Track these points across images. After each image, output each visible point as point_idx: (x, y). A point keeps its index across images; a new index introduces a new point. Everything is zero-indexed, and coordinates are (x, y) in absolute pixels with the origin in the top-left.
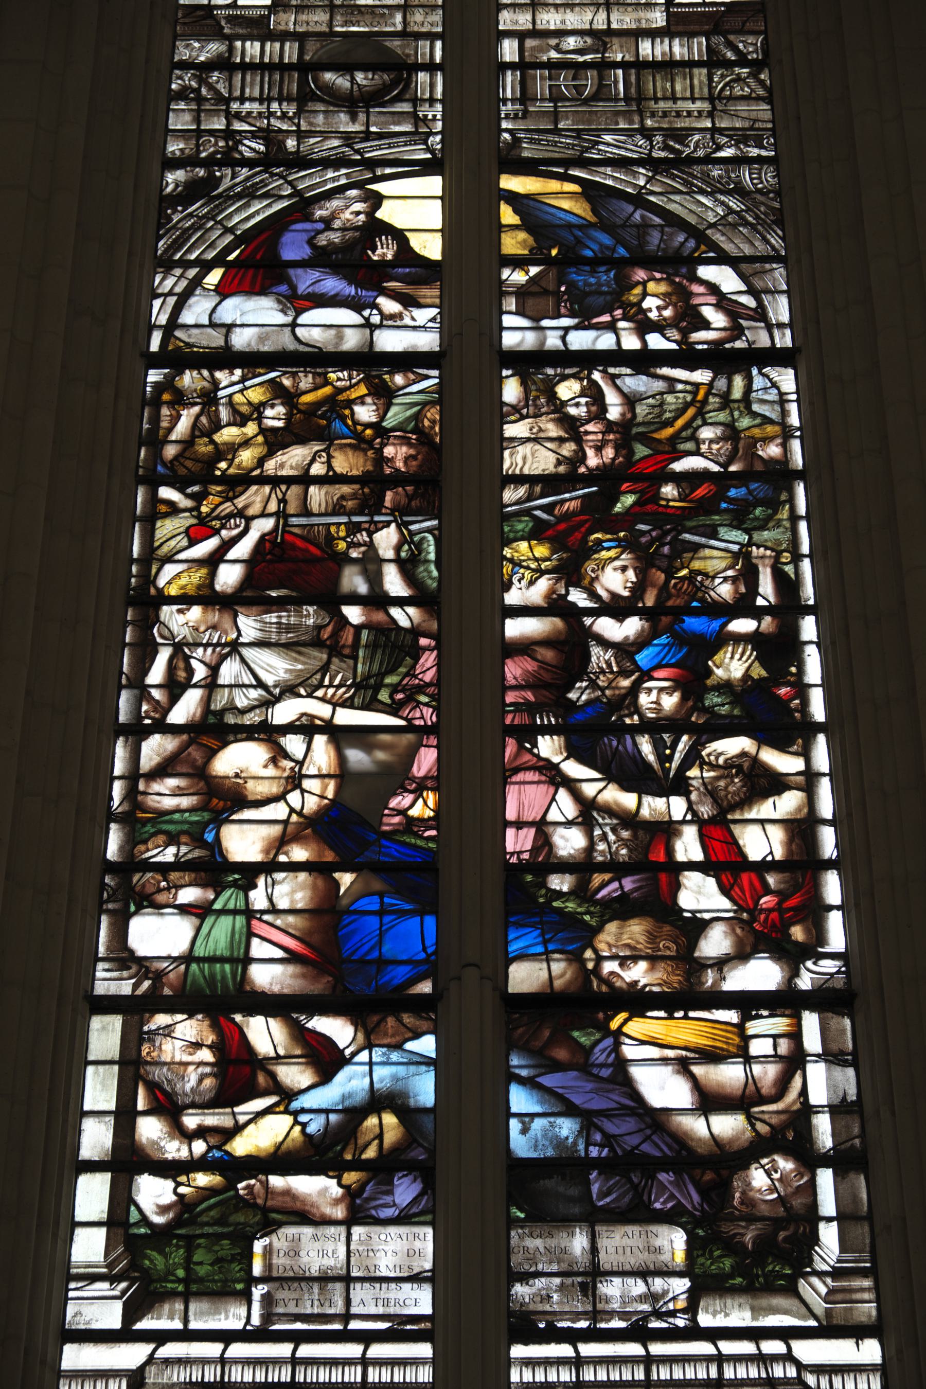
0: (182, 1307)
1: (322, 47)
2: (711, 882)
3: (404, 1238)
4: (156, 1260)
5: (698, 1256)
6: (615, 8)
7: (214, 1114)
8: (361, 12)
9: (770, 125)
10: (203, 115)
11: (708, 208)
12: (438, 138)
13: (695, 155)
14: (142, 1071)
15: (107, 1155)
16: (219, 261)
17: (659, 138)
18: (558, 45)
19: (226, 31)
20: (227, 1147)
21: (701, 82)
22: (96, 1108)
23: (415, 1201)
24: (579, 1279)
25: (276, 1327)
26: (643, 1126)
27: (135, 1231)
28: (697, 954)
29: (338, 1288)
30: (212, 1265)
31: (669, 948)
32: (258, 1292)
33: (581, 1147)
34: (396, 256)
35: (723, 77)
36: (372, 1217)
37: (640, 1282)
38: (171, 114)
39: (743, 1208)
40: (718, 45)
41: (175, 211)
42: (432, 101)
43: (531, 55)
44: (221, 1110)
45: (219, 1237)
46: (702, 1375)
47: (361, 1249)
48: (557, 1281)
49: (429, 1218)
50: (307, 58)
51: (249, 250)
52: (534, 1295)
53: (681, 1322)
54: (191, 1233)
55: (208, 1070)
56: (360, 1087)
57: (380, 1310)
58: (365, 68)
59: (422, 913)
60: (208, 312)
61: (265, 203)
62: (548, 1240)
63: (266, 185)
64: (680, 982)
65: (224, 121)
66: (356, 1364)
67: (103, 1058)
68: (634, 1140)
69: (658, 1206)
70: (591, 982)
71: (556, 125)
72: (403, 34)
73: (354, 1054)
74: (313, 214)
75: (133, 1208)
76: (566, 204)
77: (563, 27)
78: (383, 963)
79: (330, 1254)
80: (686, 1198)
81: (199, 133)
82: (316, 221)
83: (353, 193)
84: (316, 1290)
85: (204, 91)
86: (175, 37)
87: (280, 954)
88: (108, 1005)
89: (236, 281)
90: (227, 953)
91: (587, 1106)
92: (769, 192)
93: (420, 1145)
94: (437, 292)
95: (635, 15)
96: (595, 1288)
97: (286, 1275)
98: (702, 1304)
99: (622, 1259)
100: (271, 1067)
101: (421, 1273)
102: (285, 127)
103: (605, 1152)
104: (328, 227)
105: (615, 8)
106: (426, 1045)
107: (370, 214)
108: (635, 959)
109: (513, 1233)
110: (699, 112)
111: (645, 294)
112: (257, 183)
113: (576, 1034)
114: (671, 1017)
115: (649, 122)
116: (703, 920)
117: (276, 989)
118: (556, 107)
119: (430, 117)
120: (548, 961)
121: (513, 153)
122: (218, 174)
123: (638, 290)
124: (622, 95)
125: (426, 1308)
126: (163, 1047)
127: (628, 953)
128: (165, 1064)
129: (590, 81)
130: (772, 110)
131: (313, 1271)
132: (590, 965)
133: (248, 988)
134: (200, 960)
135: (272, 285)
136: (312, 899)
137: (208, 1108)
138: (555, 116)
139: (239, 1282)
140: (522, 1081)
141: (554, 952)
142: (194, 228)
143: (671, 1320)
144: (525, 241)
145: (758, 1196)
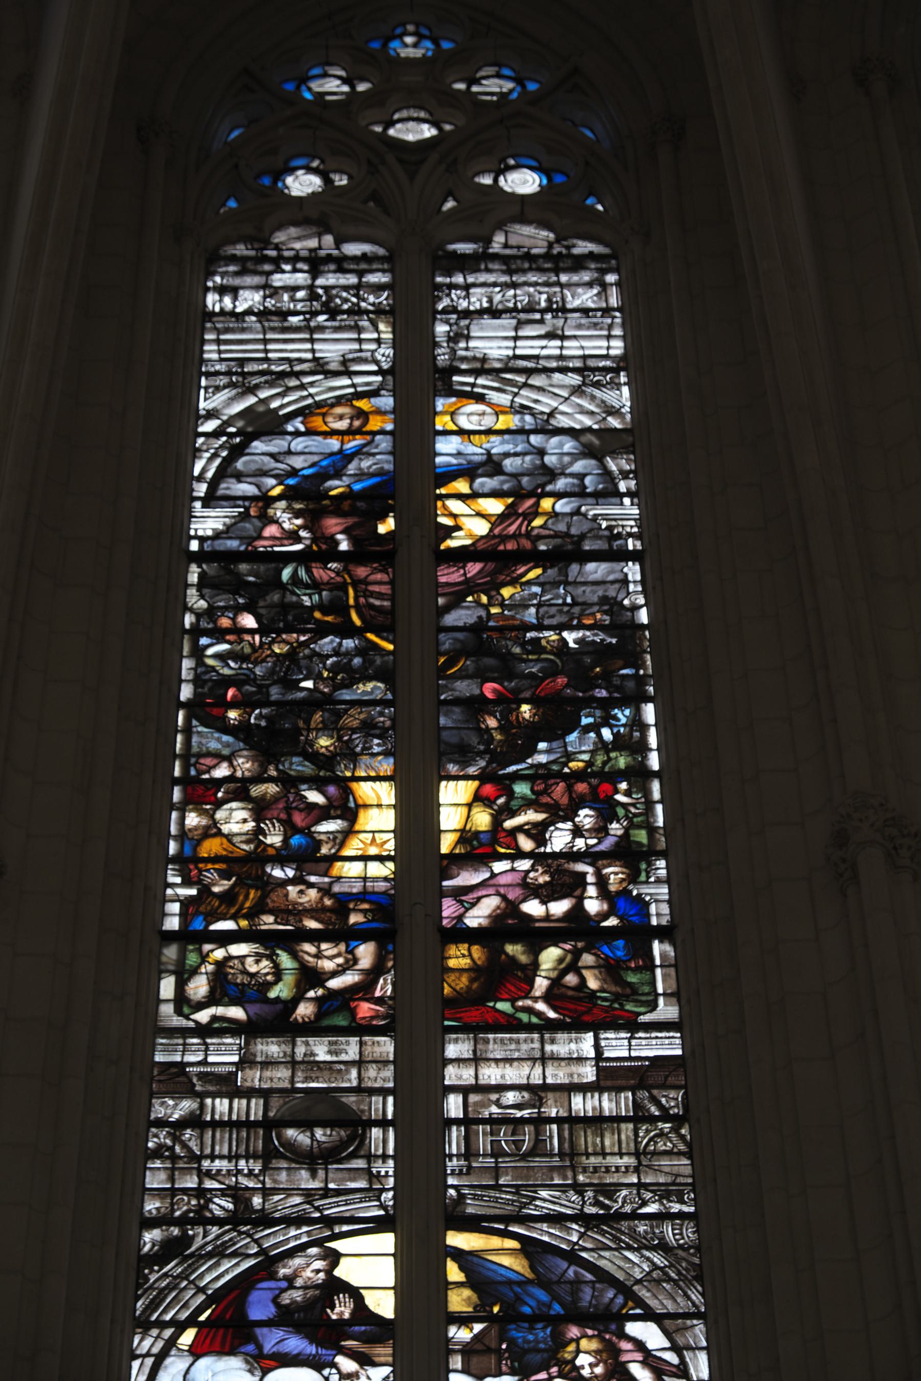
1: (285, 1103)
6: (549, 1063)
8: (320, 1069)
9: (690, 1180)
10: (176, 1173)
11: (635, 1264)
12: (390, 1194)
13: (623, 1210)
16: (191, 1321)
17: (590, 1194)
18: (498, 1100)
19: (198, 1088)
21: (627, 1137)
34: (353, 1314)
35: (647, 1131)
38: (148, 1173)
41: (152, 1271)
42: (385, 1157)
43: (475, 1111)
50: (271, 1114)
51: (219, 1310)
58: (324, 1124)
60: (183, 1373)
61: (234, 1261)
63: (234, 1244)
65: (196, 1179)
71: (497, 1181)
74: (277, 1272)
76: (506, 1261)
77: (502, 1082)
81: (173, 1191)
82: (280, 1280)
83: (313, 1251)
85: (178, 1149)
86: (152, 1095)
89: (208, 1341)
92: (690, 1247)
94: (389, 1351)
95: (568, 1070)
102: (251, 1185)
104: (291, 1286)
105: (549, 1063)
107: (329, 1272)
110: (626, 1167)
111: (578, 1351)
112: (226, 1242)
115: (581, 1178)
118: (497, 1162)
119: (383, 1173)
121: (458, 1209)
122: (190, 1232)
123: (572, 1348)
124: (556, 1151)
129: (527, 1136)
130: (692, 1164)
135: (241, 1345)
138: (496, 1172)
142: (170, 1288)
144: (469, 1298)
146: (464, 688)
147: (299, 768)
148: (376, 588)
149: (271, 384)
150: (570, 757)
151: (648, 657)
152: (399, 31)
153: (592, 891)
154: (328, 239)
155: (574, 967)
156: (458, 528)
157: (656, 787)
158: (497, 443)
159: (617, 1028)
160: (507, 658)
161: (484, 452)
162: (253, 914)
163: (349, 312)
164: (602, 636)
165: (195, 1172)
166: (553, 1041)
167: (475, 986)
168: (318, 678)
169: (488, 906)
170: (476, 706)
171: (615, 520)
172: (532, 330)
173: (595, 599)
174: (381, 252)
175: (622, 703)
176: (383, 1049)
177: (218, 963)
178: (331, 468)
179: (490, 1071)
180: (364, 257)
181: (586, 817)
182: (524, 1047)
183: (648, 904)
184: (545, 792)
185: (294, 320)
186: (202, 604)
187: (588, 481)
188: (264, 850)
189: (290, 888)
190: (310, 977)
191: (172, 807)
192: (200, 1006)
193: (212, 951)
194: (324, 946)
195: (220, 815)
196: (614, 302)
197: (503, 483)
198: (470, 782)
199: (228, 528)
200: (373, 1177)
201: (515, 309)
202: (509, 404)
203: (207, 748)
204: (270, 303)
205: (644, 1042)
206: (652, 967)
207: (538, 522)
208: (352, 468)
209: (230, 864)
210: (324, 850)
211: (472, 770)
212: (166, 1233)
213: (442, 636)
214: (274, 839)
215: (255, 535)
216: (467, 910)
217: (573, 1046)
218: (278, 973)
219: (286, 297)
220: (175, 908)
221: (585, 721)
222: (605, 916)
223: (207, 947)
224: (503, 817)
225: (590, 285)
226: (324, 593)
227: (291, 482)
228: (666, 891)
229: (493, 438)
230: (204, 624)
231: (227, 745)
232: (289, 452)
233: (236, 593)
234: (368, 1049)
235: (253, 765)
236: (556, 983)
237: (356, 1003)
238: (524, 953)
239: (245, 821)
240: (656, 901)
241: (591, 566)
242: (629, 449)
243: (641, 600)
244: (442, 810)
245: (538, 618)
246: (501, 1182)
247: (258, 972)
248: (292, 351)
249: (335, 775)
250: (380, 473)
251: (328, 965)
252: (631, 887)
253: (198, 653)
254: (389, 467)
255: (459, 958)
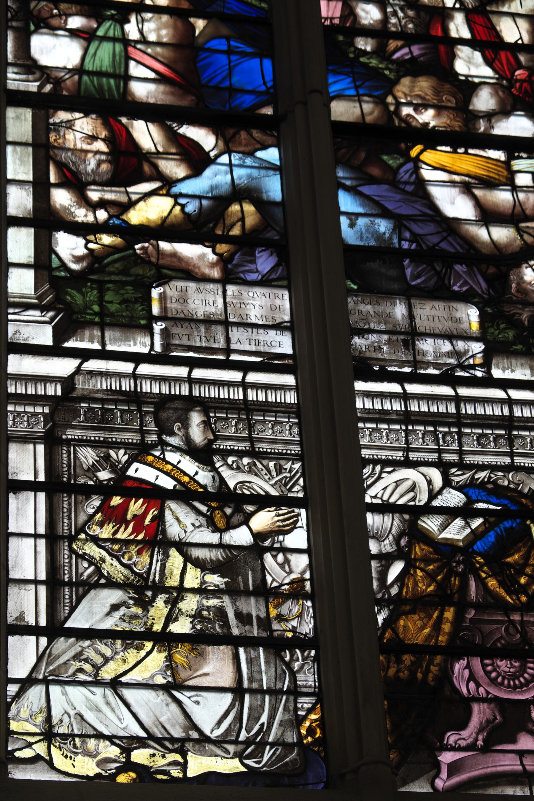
0: (99, 334)
2: (478, 56)
3: (267, 296)
4: (76, 297)
5: (489, 327)
7: (111, 191)
14: (51, 153)
15: (29, 214)
20: (124, 217)
22: (18, 177)
23: (273, 270)
24: (402, 337)
25: (174, 354)
26: (440, 230)
27: (58, 274)
28: (471, 107)
29: (219, 330)
30: (120, 304)
31: (450, 101)
32: (158, 327)
33: (395, 241)
36: (241, 279)
37: (447, 343)
39: (519, 295)
44: (117, 189)
45: (126, 283)
46: (498, 412)
47: (234, 301)
48: (385, 337)
49: (285, 283)
52: (369, 346)
53: (479, 374)
54: (101, 279)
55: (103, 157)
56: (224, 181)
57: (253, 348)
59: (261, 56)
62: (376, 306)
64: (460, 127)
66: (238, 386)
67: (19, 140)
68: (435, 239)
69: (456, 288)
70: (393, 120)
73: (217, 156)
75: (53, 256)
78: (233, 91)
79: (211, 303)
80: (476, 285)
84: (203, 329)
87: (152, 75)
88: (20, 99)
90: (110, 70)
91: (397, 211)
93: (273, 229)
96: (414, 345)
97: (178, 316)
98: (494, 362)
99: (432, 325)
100: (153, 160)
101: (282, 323)
103: (414, 246)
106: (272, 155)
108: (426, 106)
109: (349, 300)
113: (385, 158)
114: (455, 152)
116: (473, 83)
117: (152, 101)
120: (360, 102)
125: (287, 348)
126: (67, 137)
127: (419, 102)
128: (69, 149)
131: (199, 315)
132: (392, 108)
133: (130, 99)
134: (90, 73)
136: (174, 36)
137: (107, 186)
139: (143, 319)
140: (347, 189)
141: (364, 95)
143: (472, 371)
145: (529, 287)
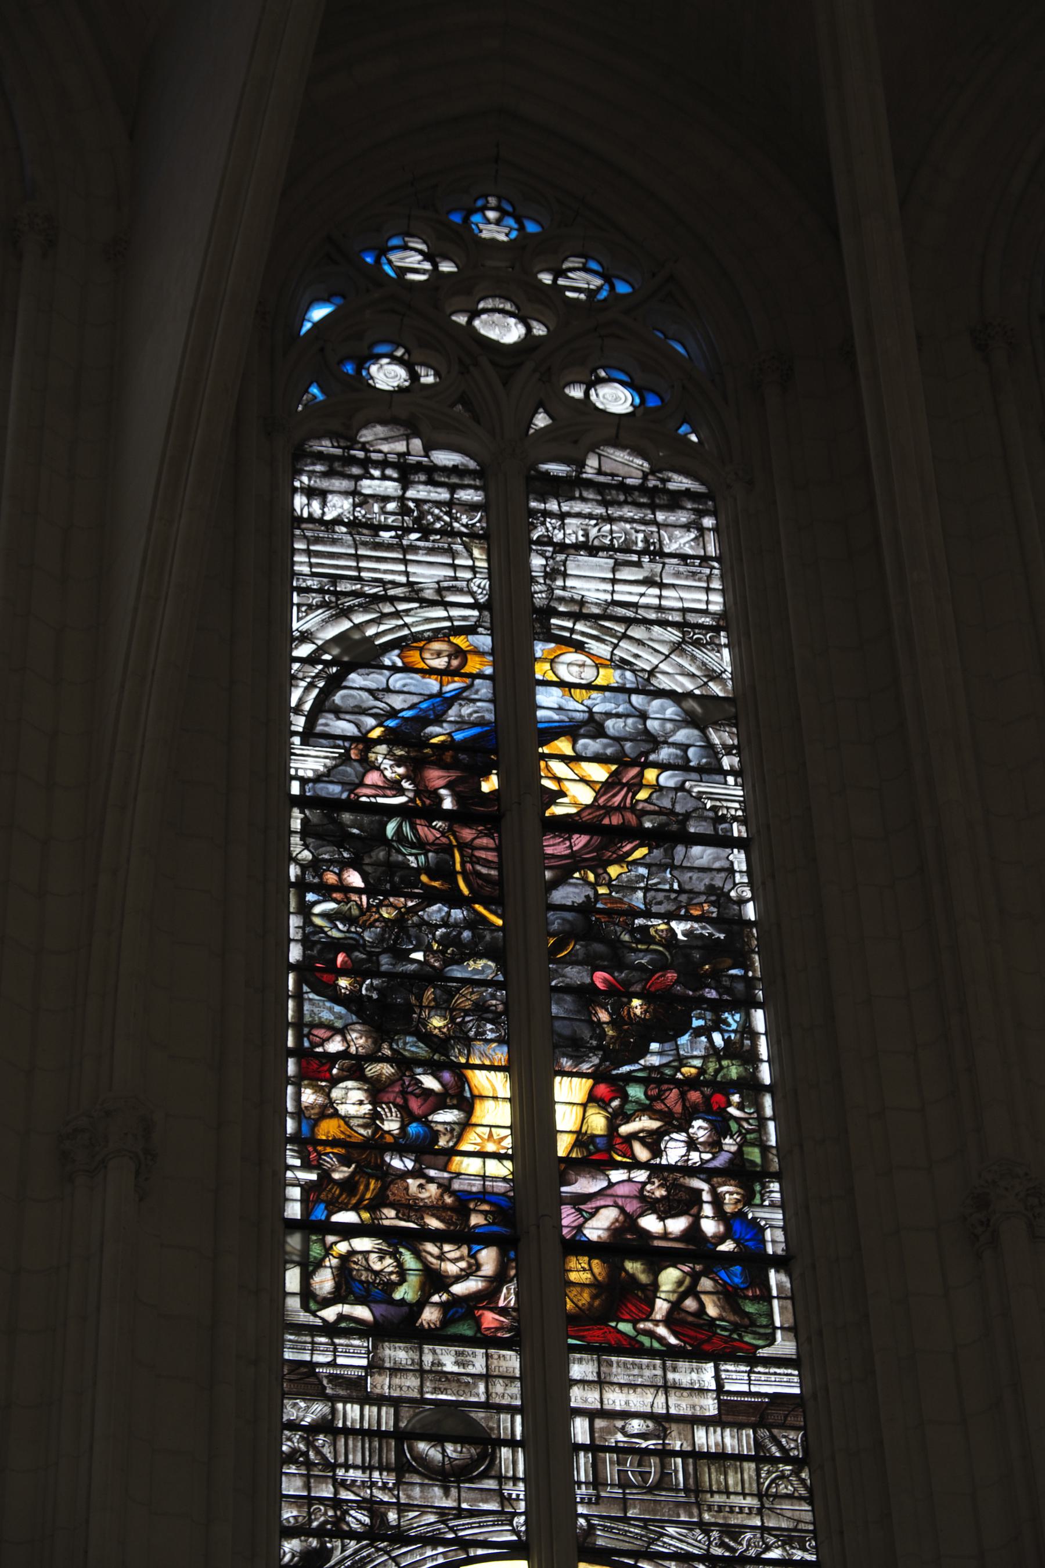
6: (672, 1392)
8: (447, 1379)
9: (811, 1527)
10: (312, 1481)
12: (522, 1519)
17: (715, 1534)
18: (623, 1427)
19: (329, 1391)
21: (750, 1477)
35: (769, 1473)
38: (284, 1478)
40: (764, 1438)
42: (515, 1479)
43: (601, 1437)
50: (402, 1425)
58: (454, 1440)
63: (372, 1561)
65: (332, 1489)
71: (625, 1513)
72: (487, 1406)
77: (627, 1409)
86: (284, 1395)
102: (386, 1499)
105: (672, 1392)
110: (750, 1508)
112: (364, 1558)
115: (706, 1516)
118: (624, 1493)
121: (588, 1540)
122: (329, 1545)
124: (682, 1486)
130: (813, 1511)
138: (624, 1503)
146: (575, 975)
147: (413, 1049)
148: (482, 854)
149: (365, 608)
150: (682, 1061)
151: (757, 957)
152: (480, 203)
153: (708, 1210)
154: (417, 444)
155: (692, 1291)
156: (562, 794)
157: (768, 1101)
158: (597, 701)
159: (737, 1360)
160: (616, 944)
161: (586, 709)
162: (375, 1206)
163: (441, 532)
164: (710, 930)
165: (330, 1481)
166: (675, 1370)
167: (597, 1303)
168: (428, 950)
169: (607, 1218)
170: (587, 996)
171: (720, 800)
172: (629, 574)
173: (701, 888)
174: (472, 465)
175: (734, 1006)
176: (509, 1364)
177: (341, 1257)
178: (431, 712)
179: (615, 1395)
180: (455, 470)
181: (700, 1128)
182: (647, 1373)
183: (763, 1230)
184: (658, 1098)
185: (386, 535)
186: (306, 855)
187: (691, 752)
188: (382, 1137)
189: (410, 1181)
190: (434, 1281)
191: (288, 1081)
192: (326, 1303)
193: (336, 1243)
194: (447, 1248)
195: (336, 1093)
196: (712, 550)
197: (606, 746)
198: (584, 1080)
199: (330, 770)
200: (506, 1500)
201: (611, 548)
202: (609, 657)
203: (320, 1018)
204: (360, 513)
205: (763, 1377)
206: (769, 1298)
207: (643, 795)
208: (452, 714)
209: (350, 1149)
210: (442, 1142)
211: (585, 1067)
212: (304, 1544)
213: (550, 914)
214: (391, 1125)
215: (357, 781)
216: (586, 1220)
217: (694, 1376)
218: (402, 1273)
219: (376, 508)
220: (295, 1192)
221: (696, 1023)
222: (721, 1239)
223: (330, 1239)
224: (618, 1122)
225: (687, 527)
226: (430, 854)
227: (391, 723)
228: (780, 1216)
229: (594, 694)
230: (309, 878)
231: (340, 1017)
232: (388, 690)
233: (340, 845)
234: (494, 1363)
235: (366, 1041)
236: (676, 1306)
237: (480, 1312)
238: (643, 1272)
239: (361, 1103)
240: (772, 1227)
241: (696, 850)
242: (733, 721)
243: (748, 894)
244: (557, 1107)
245: (645, 904)
246: (629, 1515)
247: (382, 1270)
248: (386, 572)
249: (443, 1055)
250: (481, 723)
251: (452, 1269)
252: (746, 1209)
253: (305, 910)
254: (490, 717)
255: (580, 1271)
